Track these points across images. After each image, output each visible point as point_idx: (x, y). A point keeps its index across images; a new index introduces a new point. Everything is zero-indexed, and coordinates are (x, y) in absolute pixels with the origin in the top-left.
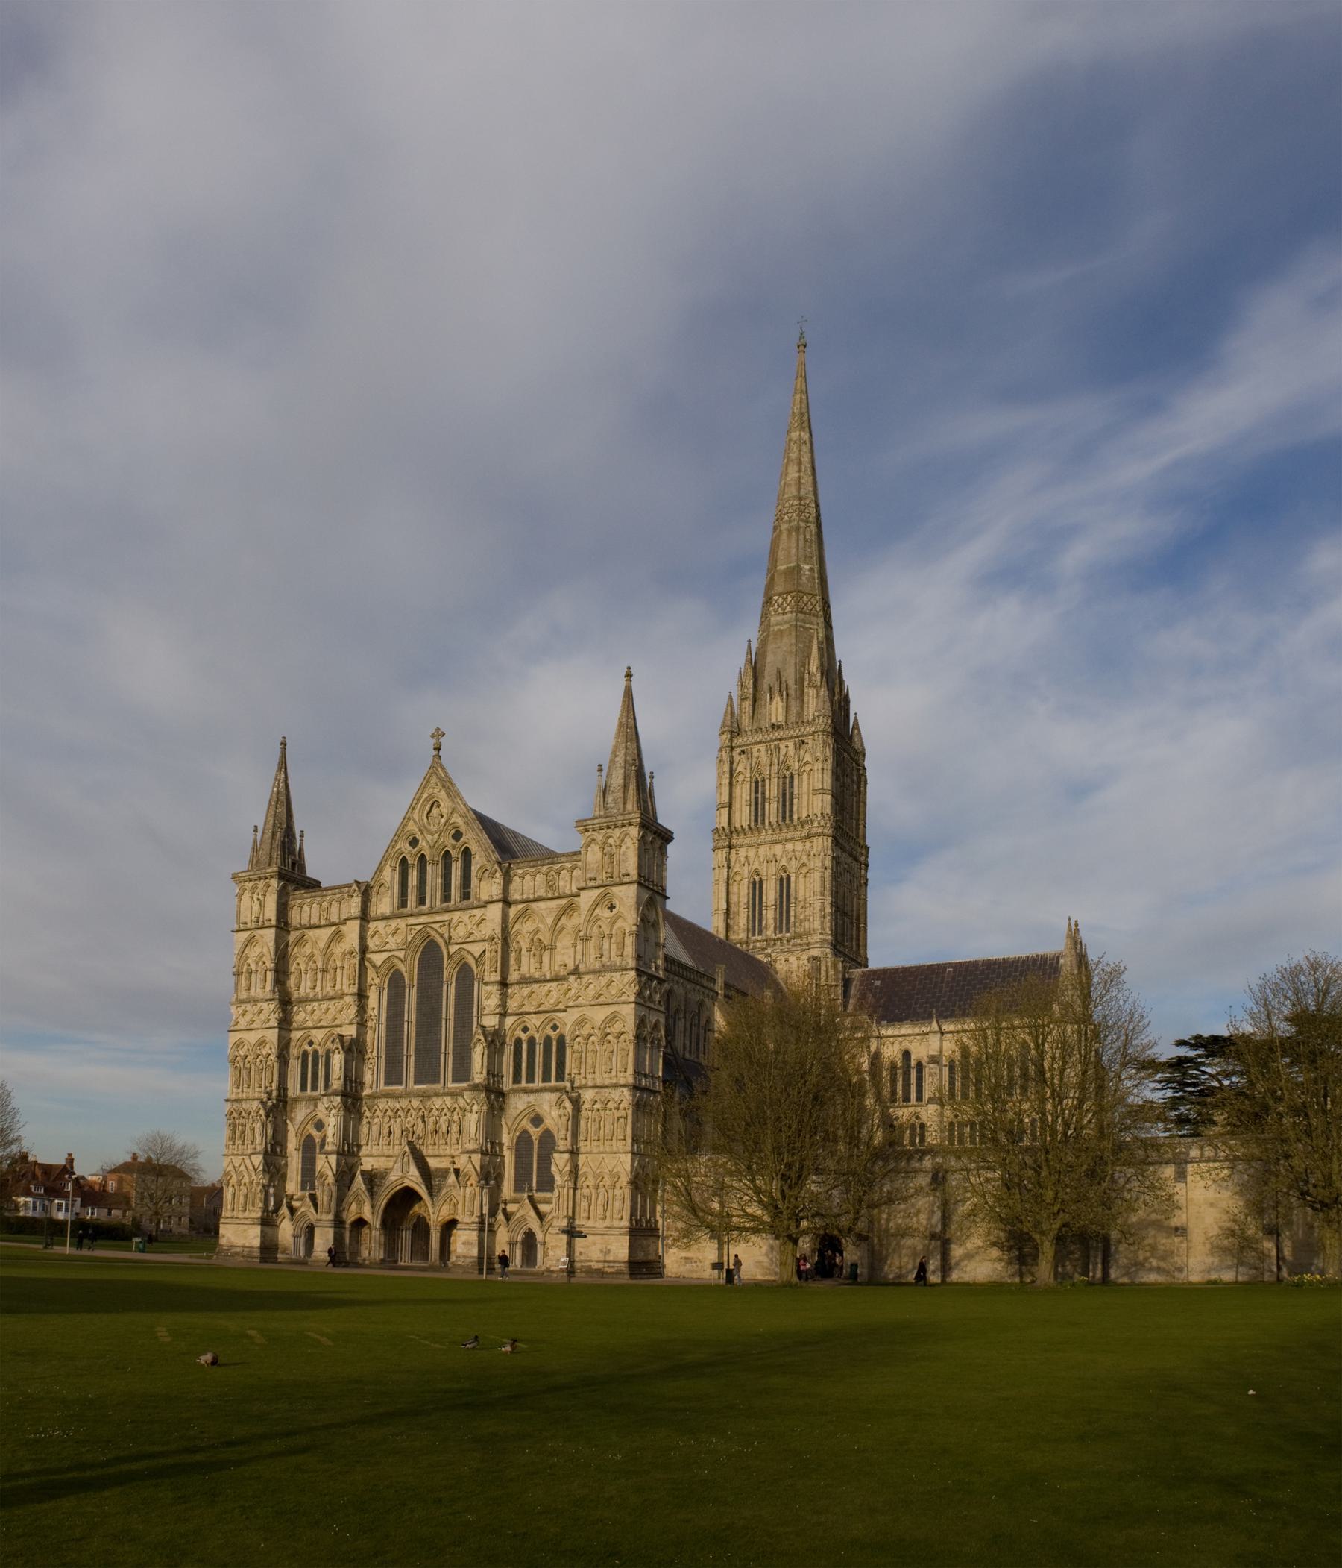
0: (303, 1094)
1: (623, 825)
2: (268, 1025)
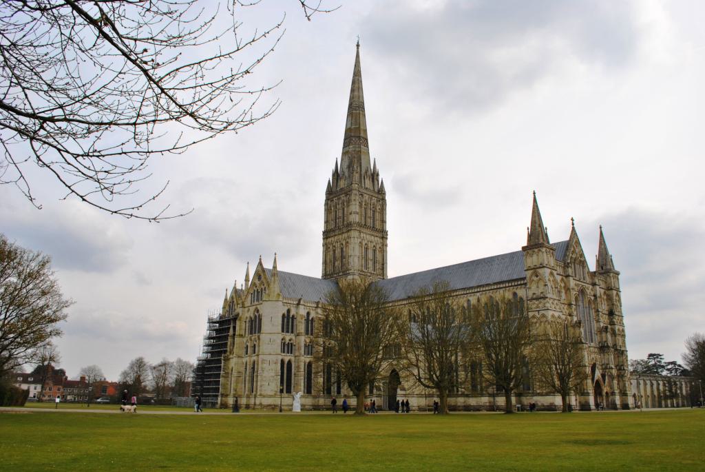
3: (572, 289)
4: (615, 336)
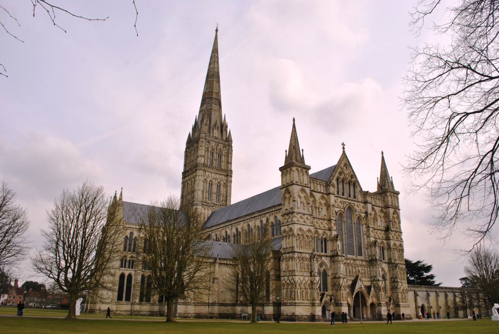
3: (333, 205)
4: (390, 251)
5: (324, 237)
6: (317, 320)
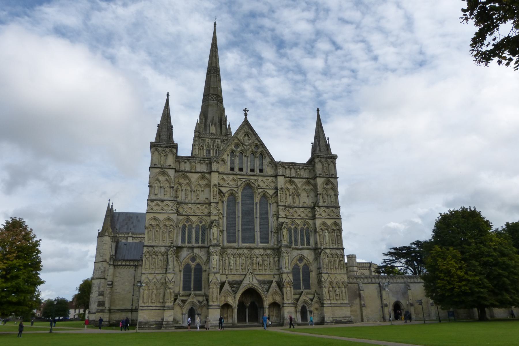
0: (183, 245)
1: (331, 158)
2: (170, 212)
5: (201, 225)
6: (164, 327)
